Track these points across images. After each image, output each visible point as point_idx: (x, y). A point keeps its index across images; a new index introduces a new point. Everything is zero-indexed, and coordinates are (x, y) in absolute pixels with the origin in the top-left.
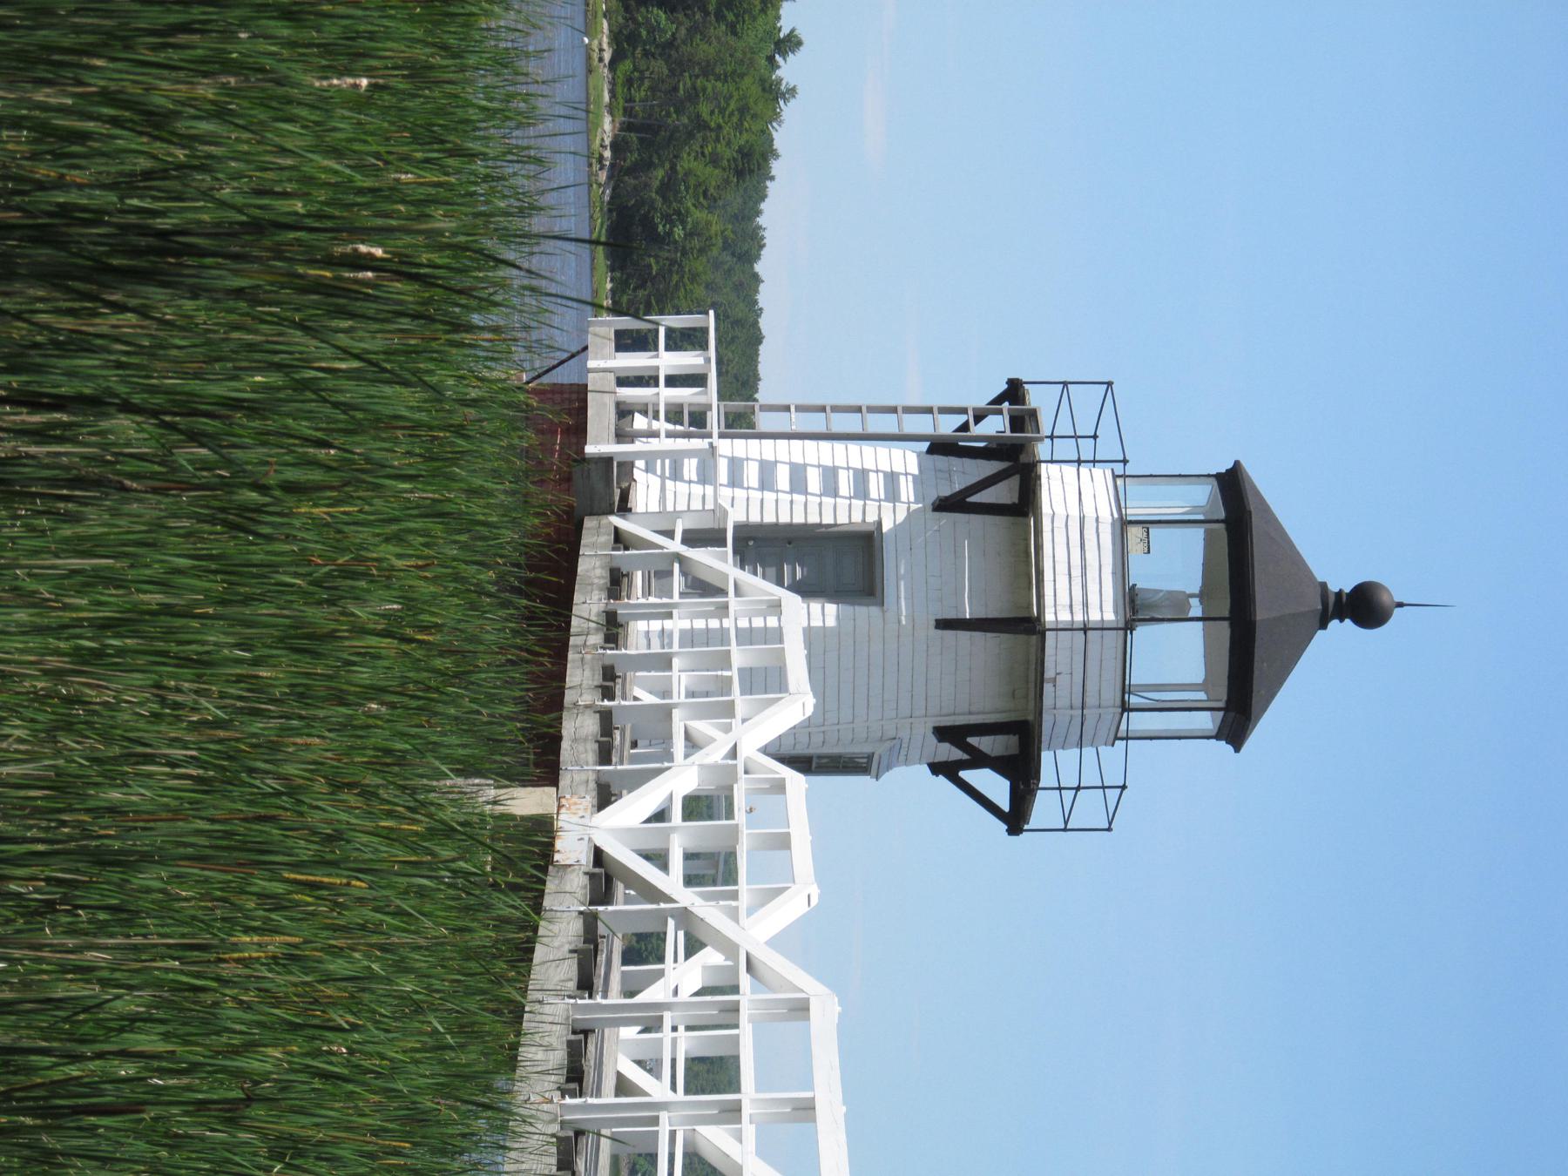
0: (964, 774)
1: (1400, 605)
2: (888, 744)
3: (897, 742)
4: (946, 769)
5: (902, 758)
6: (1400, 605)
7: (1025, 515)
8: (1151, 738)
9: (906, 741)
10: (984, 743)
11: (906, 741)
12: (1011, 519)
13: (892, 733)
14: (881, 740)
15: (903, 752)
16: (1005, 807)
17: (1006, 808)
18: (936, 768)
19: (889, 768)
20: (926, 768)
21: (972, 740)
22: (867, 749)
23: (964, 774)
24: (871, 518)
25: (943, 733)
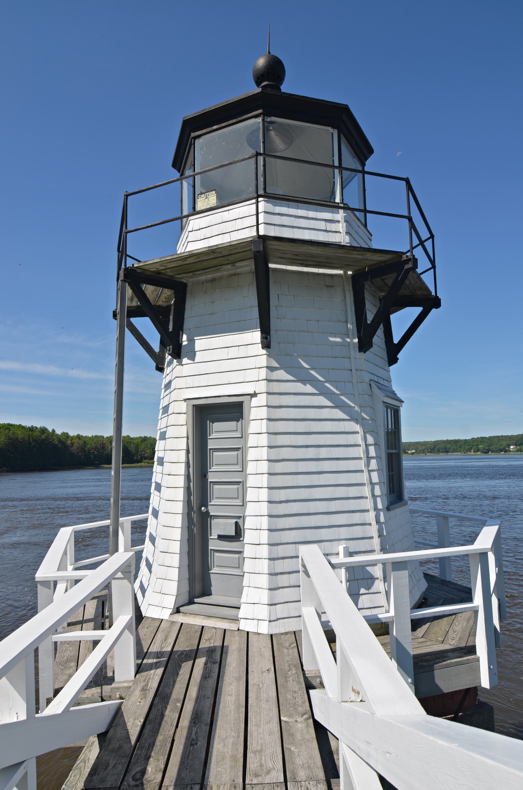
0: (396, 340)
1: (269, 53)
2: (375, 390)
3: (373, 385)
4: (393, 352)
5: (385, 383)
6: (269, 53)
7: (185, 285)
8: (364, 190)
9: (372, 377)
10: (370, 317)
11: (372, 377)
12: (188, 296)
13: (366, 386)
14: (371, 396)
15: (381, 381)
16: (419, 309)
17: (419, 309)
18: (393, 360)
19: (393, 393)
20: (392, 368)
21: (370, 317)
22: (381, 408)
23: (396, 340)
24: (183, 407)
25: (364, 345)
